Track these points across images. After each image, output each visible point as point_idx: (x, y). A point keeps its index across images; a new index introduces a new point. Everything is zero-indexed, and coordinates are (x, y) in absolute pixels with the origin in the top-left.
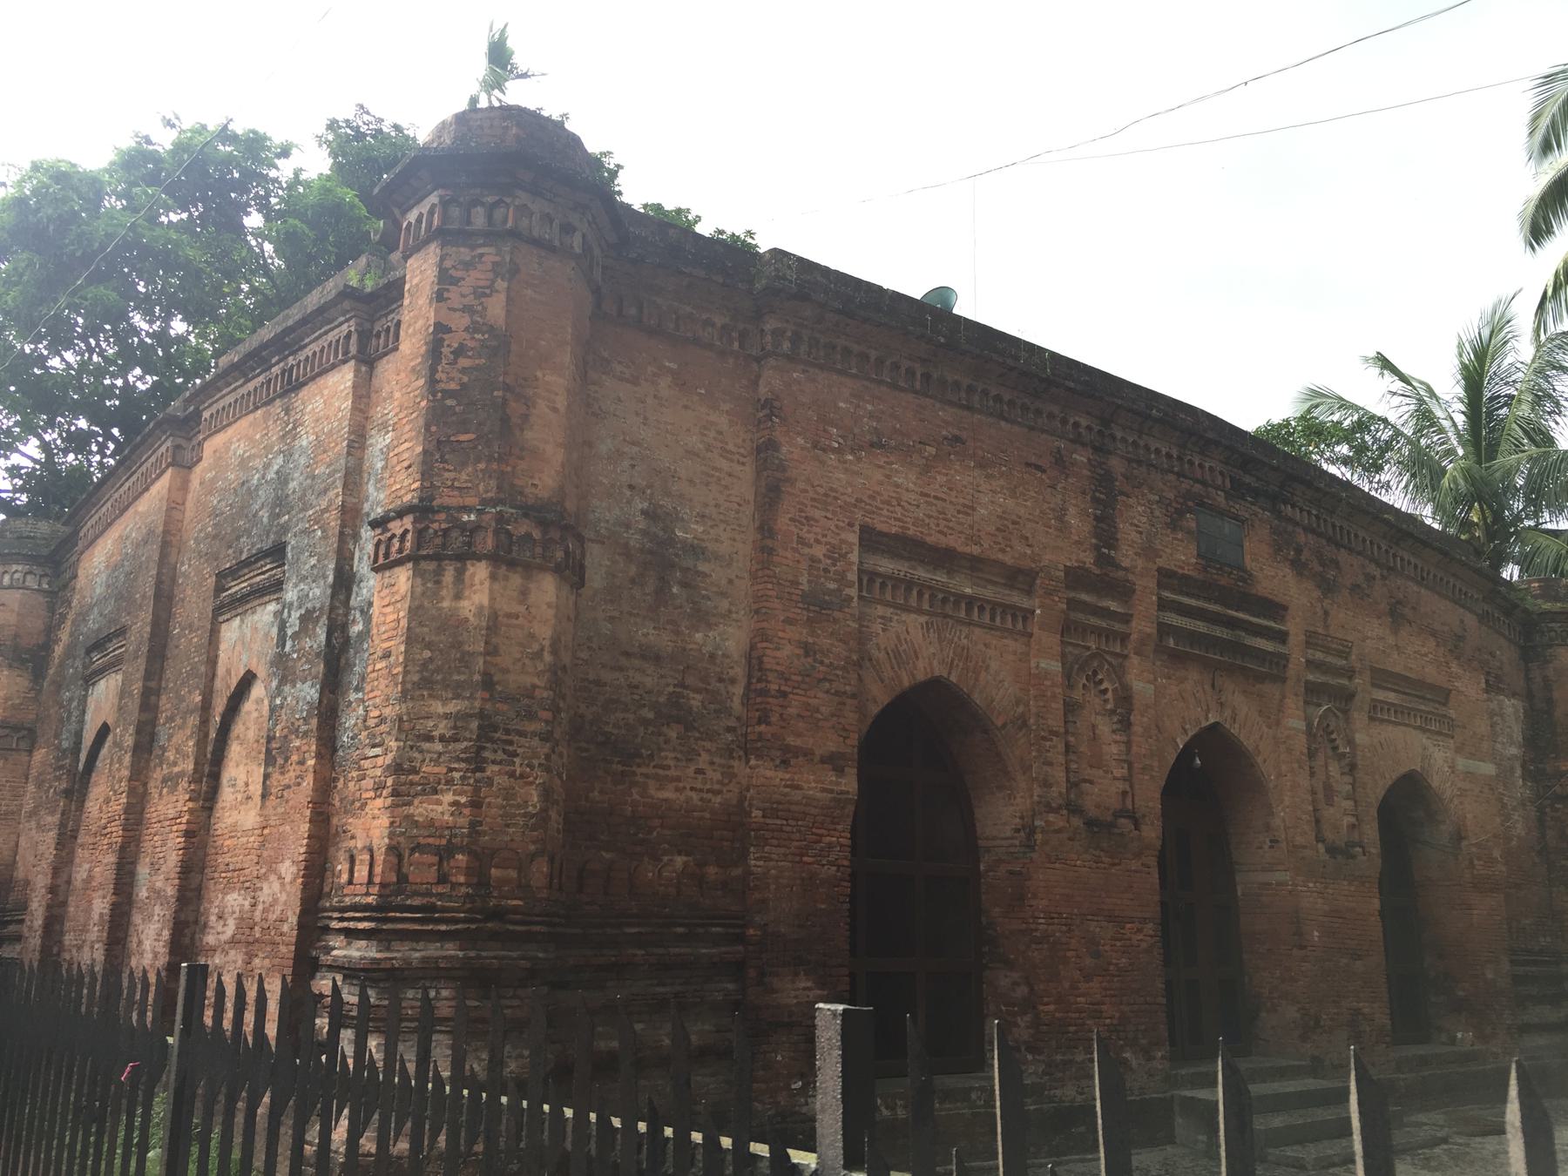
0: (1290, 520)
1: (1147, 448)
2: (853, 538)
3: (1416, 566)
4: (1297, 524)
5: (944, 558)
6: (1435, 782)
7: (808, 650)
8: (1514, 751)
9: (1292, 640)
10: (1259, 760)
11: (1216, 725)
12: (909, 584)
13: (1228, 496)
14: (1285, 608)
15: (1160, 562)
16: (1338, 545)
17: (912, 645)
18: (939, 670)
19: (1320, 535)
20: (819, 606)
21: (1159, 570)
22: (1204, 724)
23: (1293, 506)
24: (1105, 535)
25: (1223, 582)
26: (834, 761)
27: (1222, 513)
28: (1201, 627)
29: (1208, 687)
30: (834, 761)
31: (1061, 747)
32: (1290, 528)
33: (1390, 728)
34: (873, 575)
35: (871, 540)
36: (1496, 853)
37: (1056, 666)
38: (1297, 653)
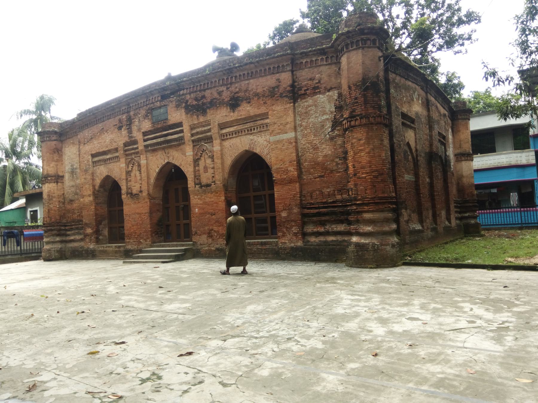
0: (183, 94)
1: (138, 104)
2: (90, 157)
3: (244, 74)
4: (186, 94)
5: (104, 153)
6: (257, 151)
7: (85, 179)
8: (325, 117)
9: (185, 131)
10: (181, 167)
11: (168, 163)
12: (100, 161)
13: (160, 101)
14: (182, 122)
15: (142, 131)
16: (204, 90)
17: (102, 171)
18: (107, 174)
19: (196, 92)
20: (86, 171)
21: (143, 133)
22: (164, 163)
23: (184, 90)
24: (130, 131)
25: (159, 126)
26: (89, 196)
27: (160, 107)
28: (155, 141)
29: (164, 154)
30: (89, 196)
31: (125, 181)
32: (183, 97)
33: (234, 139)
34: (95, 162)
35: (93, 156)
36: (291, 169)
37: (124, 165)
38: (187, 134)
